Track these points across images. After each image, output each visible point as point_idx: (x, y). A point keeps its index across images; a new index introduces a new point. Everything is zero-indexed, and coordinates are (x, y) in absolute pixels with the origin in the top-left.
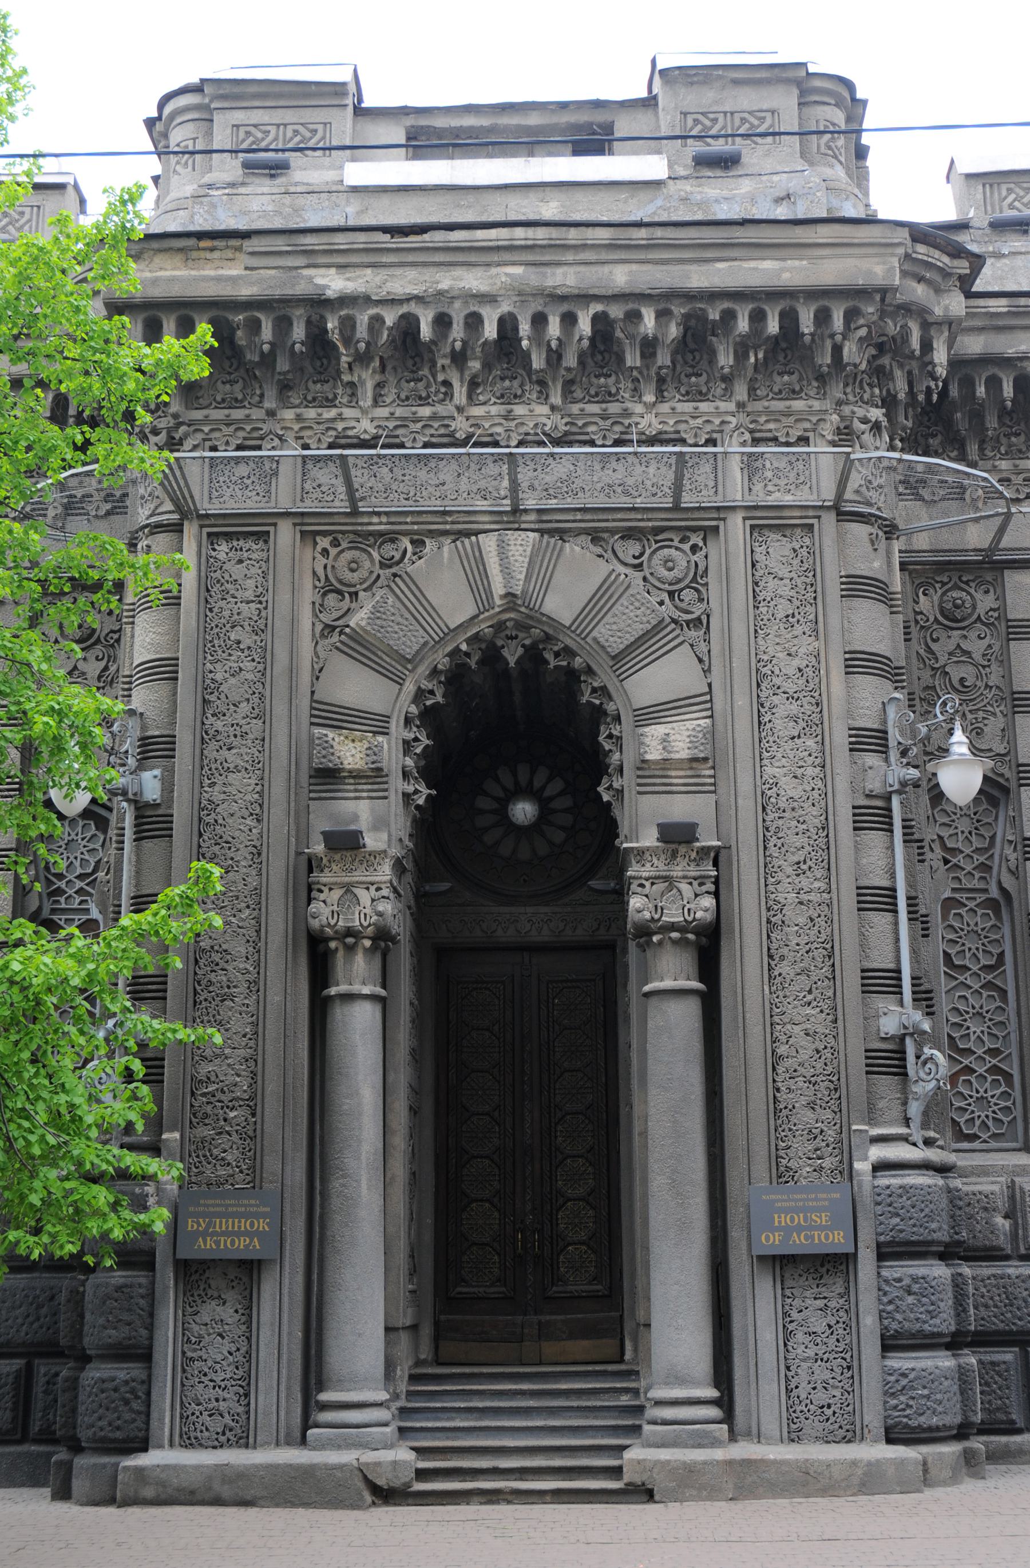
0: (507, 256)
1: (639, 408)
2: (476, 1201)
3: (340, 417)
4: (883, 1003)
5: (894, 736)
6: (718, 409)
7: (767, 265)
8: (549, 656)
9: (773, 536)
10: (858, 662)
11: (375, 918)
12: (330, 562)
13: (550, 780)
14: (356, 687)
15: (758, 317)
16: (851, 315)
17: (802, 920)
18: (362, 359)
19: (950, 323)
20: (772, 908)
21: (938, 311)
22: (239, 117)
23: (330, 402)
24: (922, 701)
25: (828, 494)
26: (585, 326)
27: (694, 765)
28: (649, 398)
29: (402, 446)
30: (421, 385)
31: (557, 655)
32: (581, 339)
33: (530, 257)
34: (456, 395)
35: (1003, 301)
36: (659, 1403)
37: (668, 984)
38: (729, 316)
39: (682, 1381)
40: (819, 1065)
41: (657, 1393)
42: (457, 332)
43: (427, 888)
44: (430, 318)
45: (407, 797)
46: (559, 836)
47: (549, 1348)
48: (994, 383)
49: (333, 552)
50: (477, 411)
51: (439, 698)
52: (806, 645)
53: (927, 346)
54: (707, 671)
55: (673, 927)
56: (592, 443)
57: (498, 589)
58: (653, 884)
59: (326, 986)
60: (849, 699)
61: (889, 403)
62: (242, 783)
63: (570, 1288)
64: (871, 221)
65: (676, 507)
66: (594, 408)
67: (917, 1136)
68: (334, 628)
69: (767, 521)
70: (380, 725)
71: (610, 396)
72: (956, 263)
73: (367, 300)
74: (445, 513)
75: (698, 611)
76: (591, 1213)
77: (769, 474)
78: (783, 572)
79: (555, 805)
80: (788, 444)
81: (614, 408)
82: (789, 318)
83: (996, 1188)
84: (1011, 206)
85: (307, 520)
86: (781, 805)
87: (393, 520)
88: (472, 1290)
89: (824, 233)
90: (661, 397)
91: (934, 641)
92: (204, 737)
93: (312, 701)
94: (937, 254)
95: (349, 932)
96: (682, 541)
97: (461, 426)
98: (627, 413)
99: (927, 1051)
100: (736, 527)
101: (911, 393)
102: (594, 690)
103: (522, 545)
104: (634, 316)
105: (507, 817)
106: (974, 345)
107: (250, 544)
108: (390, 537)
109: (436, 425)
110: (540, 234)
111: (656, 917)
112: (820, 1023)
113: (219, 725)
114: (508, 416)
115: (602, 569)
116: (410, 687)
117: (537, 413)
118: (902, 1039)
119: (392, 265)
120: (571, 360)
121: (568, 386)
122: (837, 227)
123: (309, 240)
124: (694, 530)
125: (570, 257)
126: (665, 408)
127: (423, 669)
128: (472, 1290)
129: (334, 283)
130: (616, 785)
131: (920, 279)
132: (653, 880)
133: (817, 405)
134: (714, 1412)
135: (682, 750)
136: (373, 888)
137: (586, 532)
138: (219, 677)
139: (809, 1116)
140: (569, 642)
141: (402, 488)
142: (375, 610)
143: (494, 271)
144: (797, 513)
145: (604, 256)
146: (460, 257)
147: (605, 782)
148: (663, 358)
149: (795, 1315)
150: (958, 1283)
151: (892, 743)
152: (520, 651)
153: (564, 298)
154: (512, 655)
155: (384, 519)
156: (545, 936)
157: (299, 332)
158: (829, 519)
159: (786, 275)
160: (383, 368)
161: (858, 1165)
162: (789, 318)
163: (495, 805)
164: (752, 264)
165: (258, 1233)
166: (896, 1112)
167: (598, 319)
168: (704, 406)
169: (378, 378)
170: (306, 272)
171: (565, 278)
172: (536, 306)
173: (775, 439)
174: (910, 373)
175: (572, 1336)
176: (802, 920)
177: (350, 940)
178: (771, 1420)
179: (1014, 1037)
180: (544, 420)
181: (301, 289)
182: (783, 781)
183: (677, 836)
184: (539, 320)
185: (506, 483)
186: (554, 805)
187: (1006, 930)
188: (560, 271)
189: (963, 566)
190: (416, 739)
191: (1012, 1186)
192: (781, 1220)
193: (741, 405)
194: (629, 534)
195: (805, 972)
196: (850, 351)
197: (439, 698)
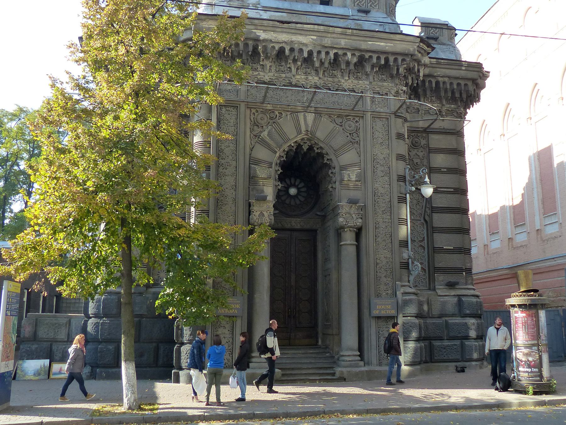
0: (312, 33)
1: (343, 81)
3: (259, 74)
4: (404, 250)
5: (408, 178)
6: (363, 84)
7: (382, 44)
8: (315, 149)
10: (400, 157)
12: (255, 117)
14: (262, 153)
15: (378, 58)
16: (403, 60)
17: (384, 227)
18: (267, 57)
19: (425, 65)
23: (256, 70)
24: (415, 168)
25: (393, 109)
26: (332, 55)
27: (357, 183)
28: (347, 78)
29: (275, 85)
30: (282, 67)
31: (318, 149)
32: (330, 60)
33: (318, 34)
34: (293, 71)
35: (435, 60)
36: (343, 356)
37: (348, 242)
38: (371, 57)
39: (352, 350)
40: (388, 266)
41: (341, 354)
42: (296, 54)
44: (289, 48)
45: (276, 186)
48: (430, 82)
49: (256, 114)
50: (298, 77)
51: (285, 159)
52: (386, 151)
55: (351, 227)
56: (330, 89)
57: (303, 129)
61: (407, 85)
62: (230, 180)
64: (401, 34)
65: (353, 110)
66: (331, 79)
67: (412, 286)
68: (256, 136)
69: (376, 116)
70: (270, 165)
71: (334, 76)
72: (428, 49)
73: (271, 41)
74: (288, 105)
75: (357, 139)
77: (377, 103)
80: (382, 95)
81: (336, 80)
82: (387, 60)
83: (424, 299)
84: (432, 33)
85: (249, 104)
86: (379, 195)
87: (274, 106)
91: (410, 151)
92: (218, 165)
93: (250, 157)
94: (425, 46)
96: (354, 119)
97: (294, 82)
98: (339, 81)
99: (416, 263)
101: (412, 84)
102: (328, 160)
104: (345, 54)
107: (231, 109)
109: (286, 79)
110: (322, 27)
112: (389, 255)
113: (223, 161)
114: (307, 79)
115: (332, 125)
116: (278, 155)
117: (314, 79)
118: (408, 259)
119: (279, 32)
120: (326, 65)
121: (324, 71)
122: (402, 36)
123: (256, 21)
124: (357, 116)
125: (329, 35)
126: (350, 81)
127: (282, 150)
129: (263, 35)
130: (334, 187)
131: (420, 52)
132: (346, 213)
133: (390, 85)
134: (359, 358)
135: (353, 178)
137: (327, 114)
138: (223, 148)
139: (385, 279)
140: (322, 145)
141: (276, 97)
142: (269, 132)
143: (308, 37)
144: (384, 114)
145: (339, 36)
146: (299, 32)
147: (330, 186)
148: (352, 67)
149: (381, 332)
151: (407, 179)
152: (308, 147)
153: (326, 47)
154: (305, 147)
155: (271, 105)
156: (298, 227)
157: (251, 48)
158: (393, 116)
159: (387, 48)
161: (398, 293)
162: (387, 60)
164: (378, 43)
165: (236, 309)
166: (407, 279)
167: (336, 54)
168: (360, 82)
169: (270, 64)
170: (254, 31)
171: (327, 42)
172: (319, 48)
173: (379, 93)
174: (412, 78)
176: (384, 227)
178: (374, 360)
179: (427, 260)
180: (317, 81)
181: (252, 36)
182: (380, 188)
183: (353, 202)
184: (319, 52)
185: (305, 99)
187: (425, 231)
188: (326, 39)
189: (418, 132)
190: (278, 170)
191: (428, 299)
193: (371, 83)
195: (384, 240)
196: (401, 70)
197: (285, 159)
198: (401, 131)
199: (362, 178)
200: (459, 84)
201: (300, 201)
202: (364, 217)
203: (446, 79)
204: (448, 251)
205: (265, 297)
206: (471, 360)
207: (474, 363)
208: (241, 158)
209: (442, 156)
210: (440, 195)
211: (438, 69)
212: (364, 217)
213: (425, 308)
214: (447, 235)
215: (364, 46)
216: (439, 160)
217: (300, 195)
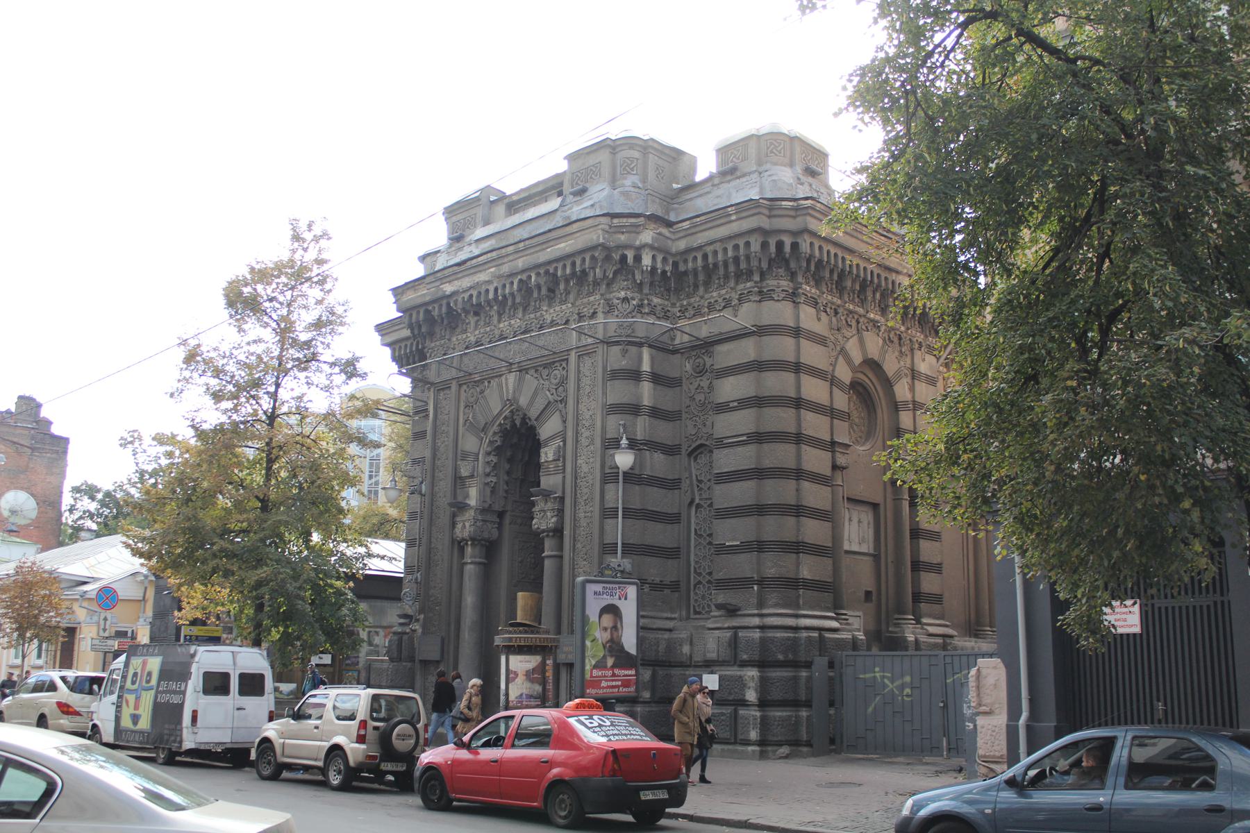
7: (563, 245)
9: (586, 358)
14: (470, 443)
15: (564, 267)
16: (593, 258)
20: (575, 519)
21: (638, 243)
22: (454, 219)
23: (465, 331)
26: (515, 286)
38: (556, 269)
48: (695, 258)
53: (638, 259)
54: (564, 422)
55: (543, 531)
60: (604, 428)
78: (588, 374)
89: (575, 227)
90: (550, 306)
95: (463, 539)
98: (542, 315)
100: (573, 357)
103: (512, 378)
106: (682, 245)
108: (481, 381)
110: (494, 254)
114: (510, 325)
129: (448, 289)
145: (516, 256)
148: (544, 291)
150: (654, 676)
154: (518, 423)
157: (444, 310)
160: (476, 314)
167: (521, 280)
171: (505, 269)
181: (440, 294)
184: (504, 286)
192: (566, 649)
194: (545, 366)
198: (616, 367)
199: (560, 456)
200: (736, 247)
202: (560, 512)
203: (718, 246)
204: (733, 550)
206: (747, 743)
207: (750, 748)
208: (451, 456)
209: (731, 378)
210: (726, 451)
211: (699, 235)
212: (560, 512)
213: (686, 649)
214: (733, 521)
215: (543, 257)
216: (730, 388)
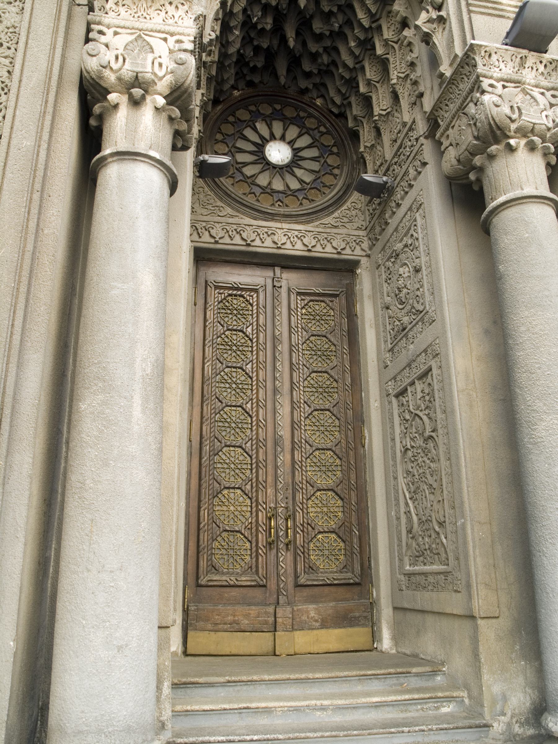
2: (228, 488)
11: (172, 66)
13: (300, 136)
43: (206, 157)
46: (308, 178)
47: (302, 640)
58: (504, 87)
59: (98, 148)
63: (321, 576)
76: (340, 502)
79: (303, 154)
88: (224, 578)
95: (137, 81)
105: (264, 158)
111: (514, 117)
128: (224, 578)
136: (171, 40)
163: (252, 148)
175: (324, 625)
177: (137, 92)
186: (303, 154)
201: (301, 181)
205: (137, 412)
217: (300, 167)
